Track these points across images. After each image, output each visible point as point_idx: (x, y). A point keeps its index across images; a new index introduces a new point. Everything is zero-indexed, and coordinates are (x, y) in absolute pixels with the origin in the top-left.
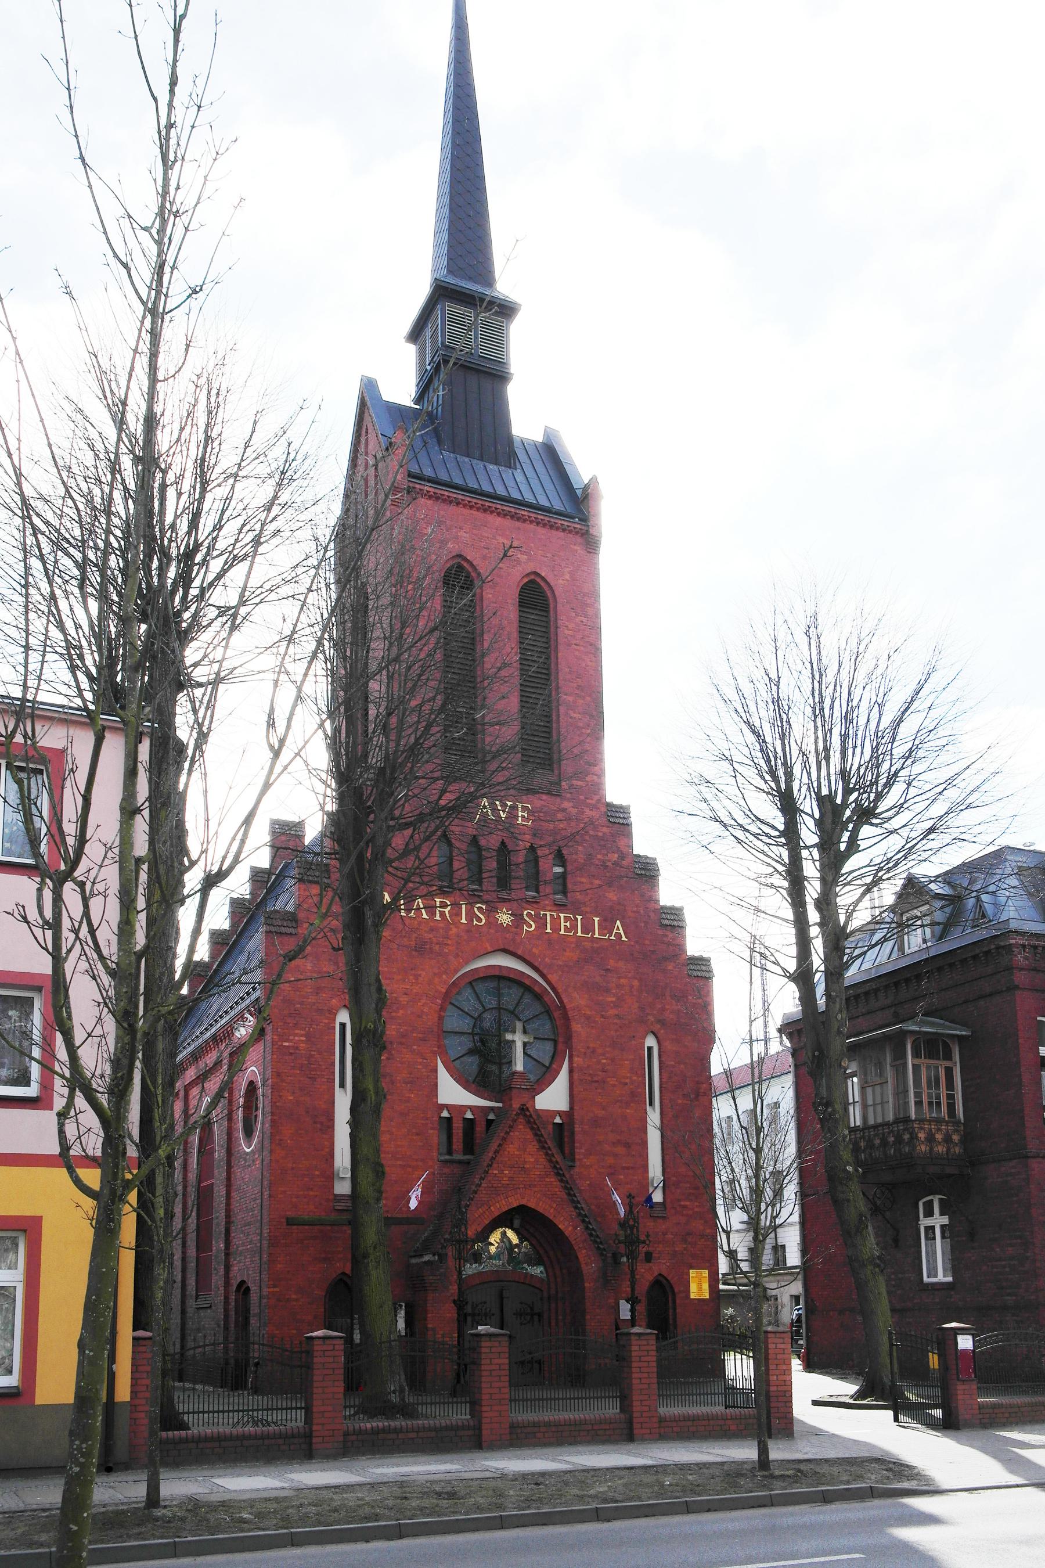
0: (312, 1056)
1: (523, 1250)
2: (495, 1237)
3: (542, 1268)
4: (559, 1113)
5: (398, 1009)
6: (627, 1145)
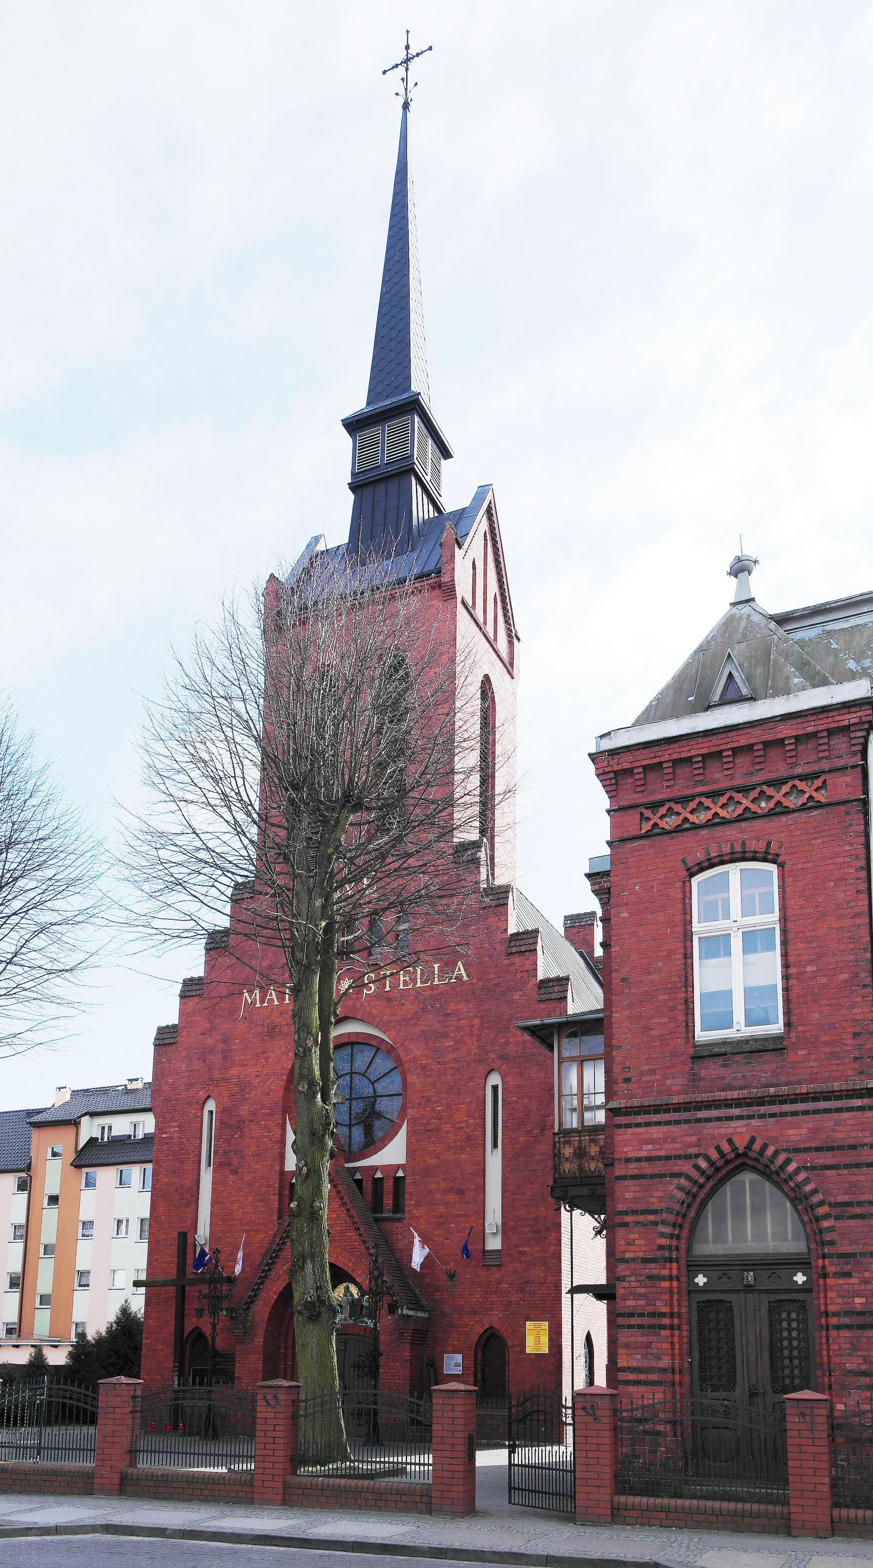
0: (182, 1143)
4: (398, 1167)
5: (251, 1090)
6: (460, 1192)
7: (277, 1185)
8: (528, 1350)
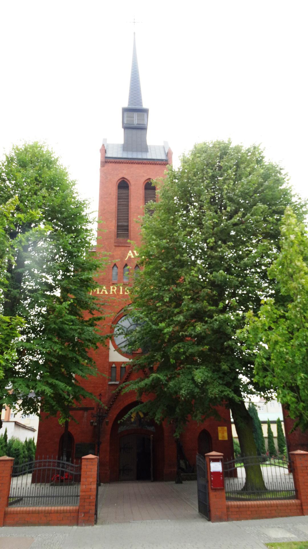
7: (108, 367)
8: (220, 439)
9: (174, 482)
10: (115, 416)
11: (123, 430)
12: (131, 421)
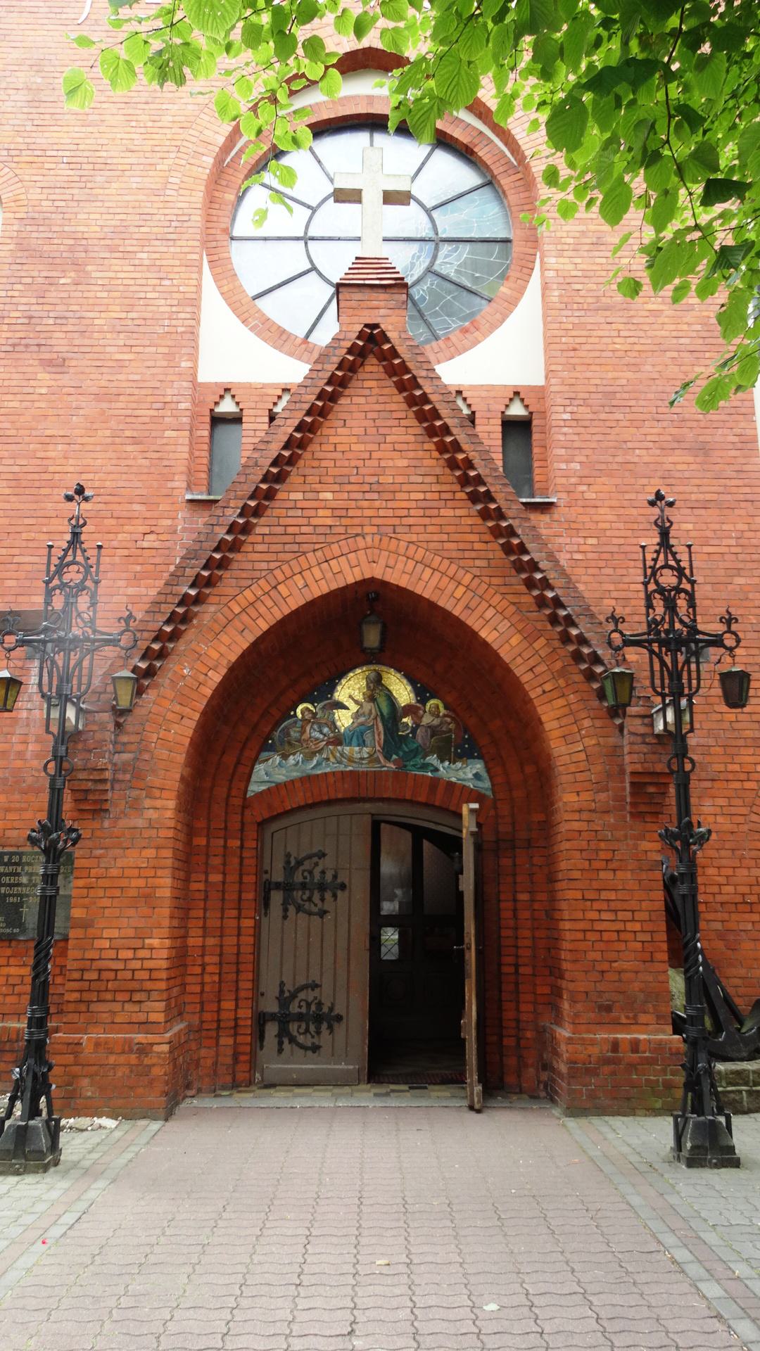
1: (427, 720)
2: (351, 689)
3: (478, 766)
9: (657, 1133)
10: (216, 677)
11: (281, 777)
12: (333, 725)
